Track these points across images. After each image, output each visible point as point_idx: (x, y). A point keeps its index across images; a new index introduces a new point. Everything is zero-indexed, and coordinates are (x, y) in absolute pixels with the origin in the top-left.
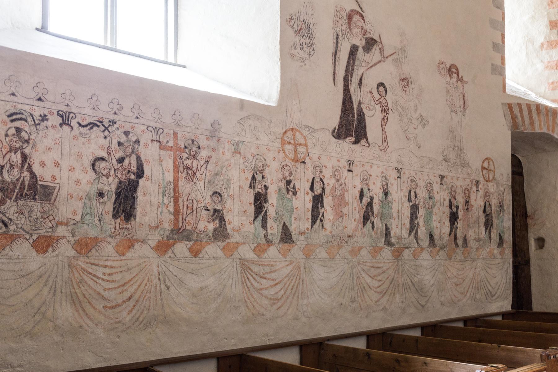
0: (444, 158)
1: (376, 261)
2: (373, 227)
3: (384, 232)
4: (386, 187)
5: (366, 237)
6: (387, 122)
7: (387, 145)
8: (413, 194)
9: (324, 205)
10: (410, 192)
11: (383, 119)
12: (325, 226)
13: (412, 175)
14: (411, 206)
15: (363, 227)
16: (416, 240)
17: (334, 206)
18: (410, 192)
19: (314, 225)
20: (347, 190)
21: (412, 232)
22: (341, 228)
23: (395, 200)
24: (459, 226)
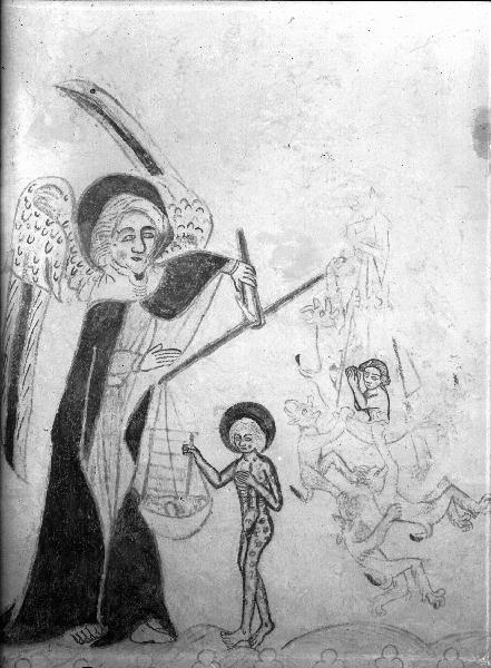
6: (269, 540)
11: (252, 530)
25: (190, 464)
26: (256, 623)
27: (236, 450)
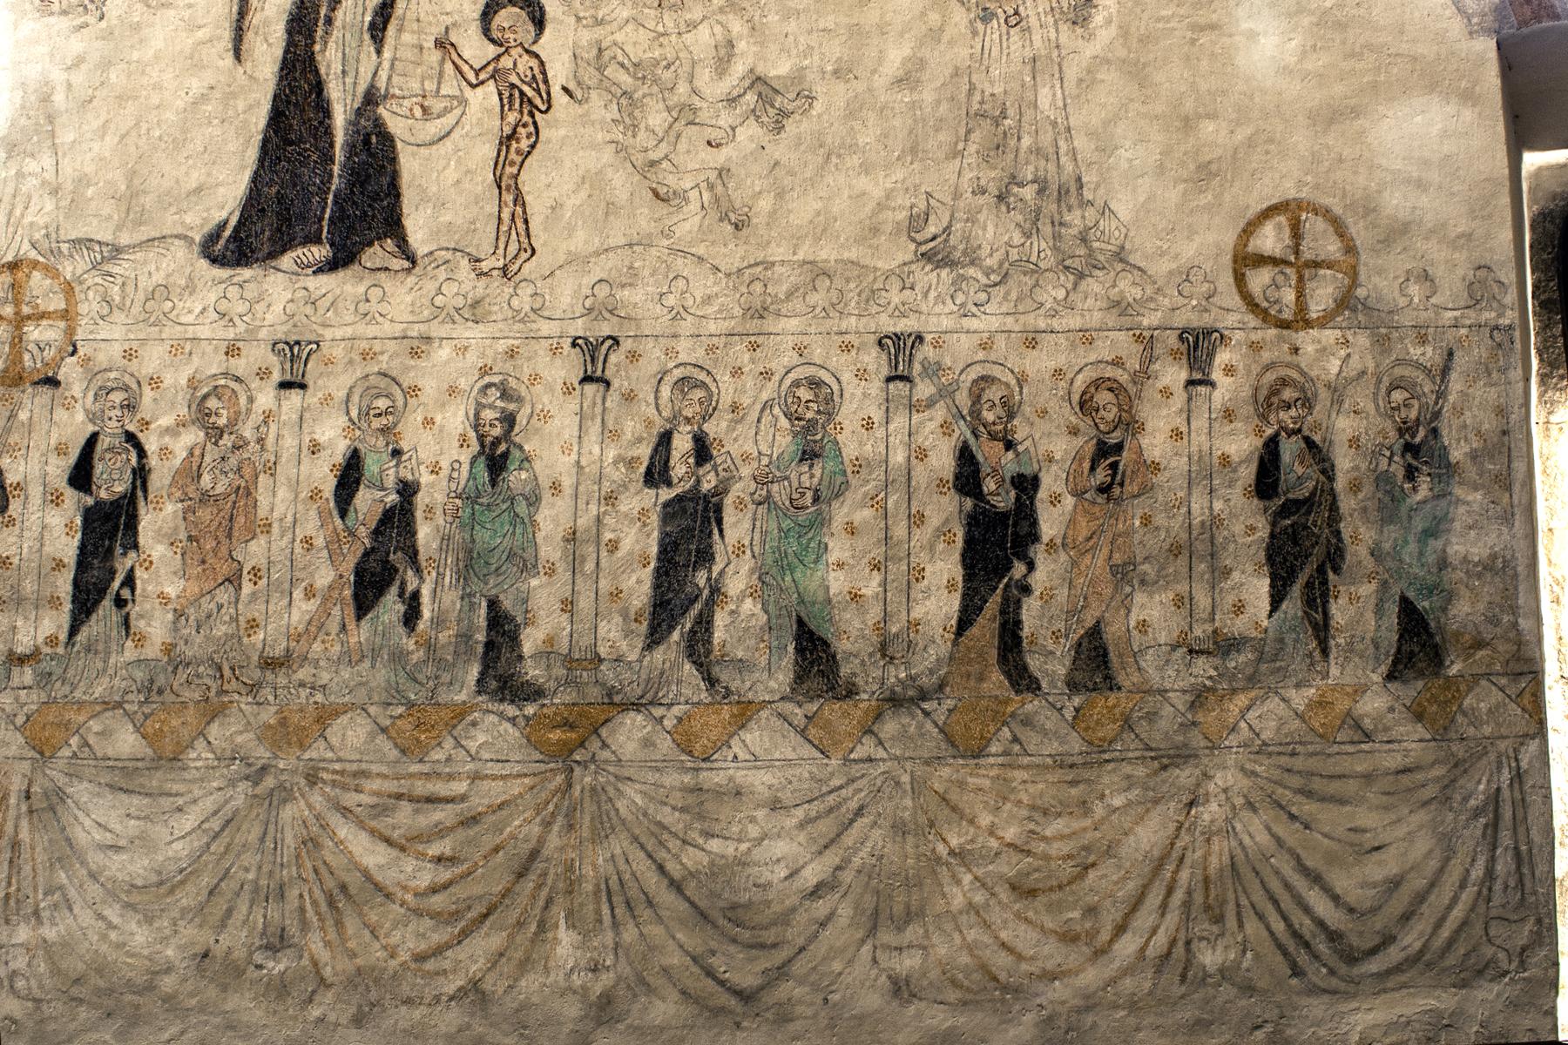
0: (924, 248)
1: (425, 768)
2: (411, 616)
3: (481, 637)
4: (497, 431)
5: (367, 664)
6: (533, 146)
7: (525, 245)
8: (682, 444)
9: (142, 541)
10: (665, 439)
11: (513, 136)
12: (138, 625)
13: (683, 357)
14: (666, 505)
15: (359, 618)
16: (699, 665)
17: (190, 538)
18: (665, 439)
19: (83, 622)
20: (271, 470)
21: (671, 628)
22: (221, 630)
23: (556, 487)
24: (1039, 579)
25: (443, 61)
26: (513, 248)
27: (501, 45)
